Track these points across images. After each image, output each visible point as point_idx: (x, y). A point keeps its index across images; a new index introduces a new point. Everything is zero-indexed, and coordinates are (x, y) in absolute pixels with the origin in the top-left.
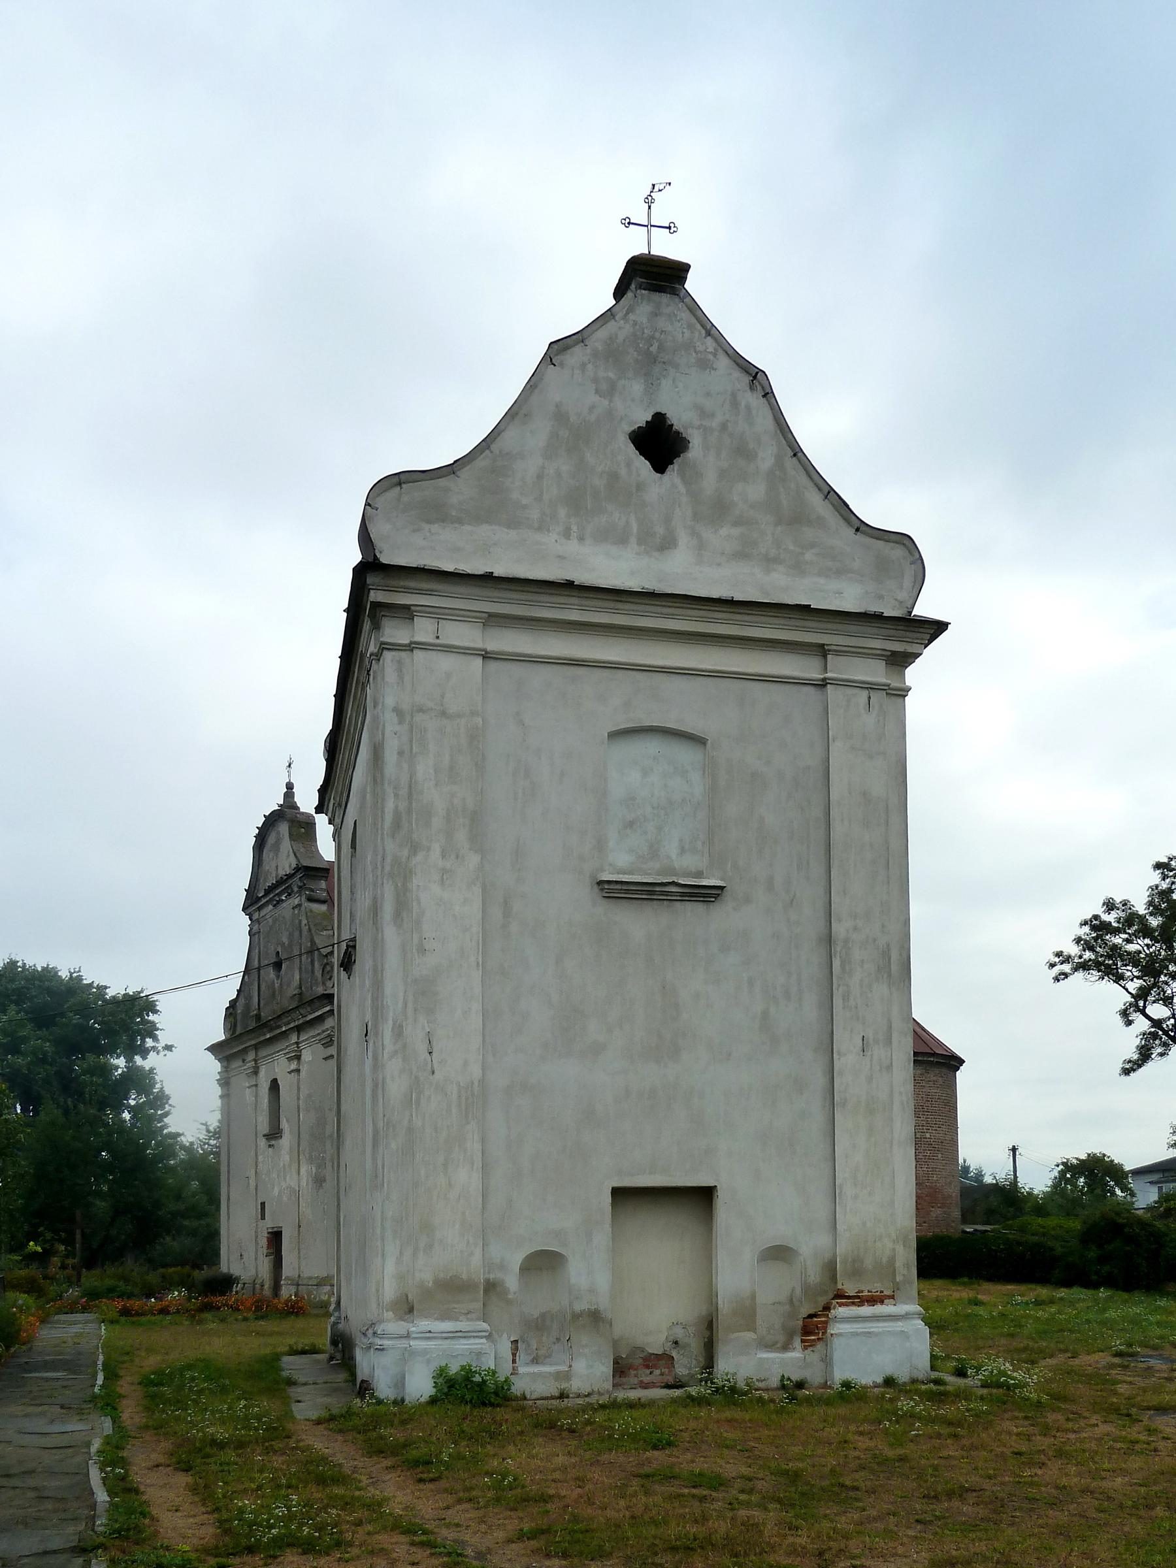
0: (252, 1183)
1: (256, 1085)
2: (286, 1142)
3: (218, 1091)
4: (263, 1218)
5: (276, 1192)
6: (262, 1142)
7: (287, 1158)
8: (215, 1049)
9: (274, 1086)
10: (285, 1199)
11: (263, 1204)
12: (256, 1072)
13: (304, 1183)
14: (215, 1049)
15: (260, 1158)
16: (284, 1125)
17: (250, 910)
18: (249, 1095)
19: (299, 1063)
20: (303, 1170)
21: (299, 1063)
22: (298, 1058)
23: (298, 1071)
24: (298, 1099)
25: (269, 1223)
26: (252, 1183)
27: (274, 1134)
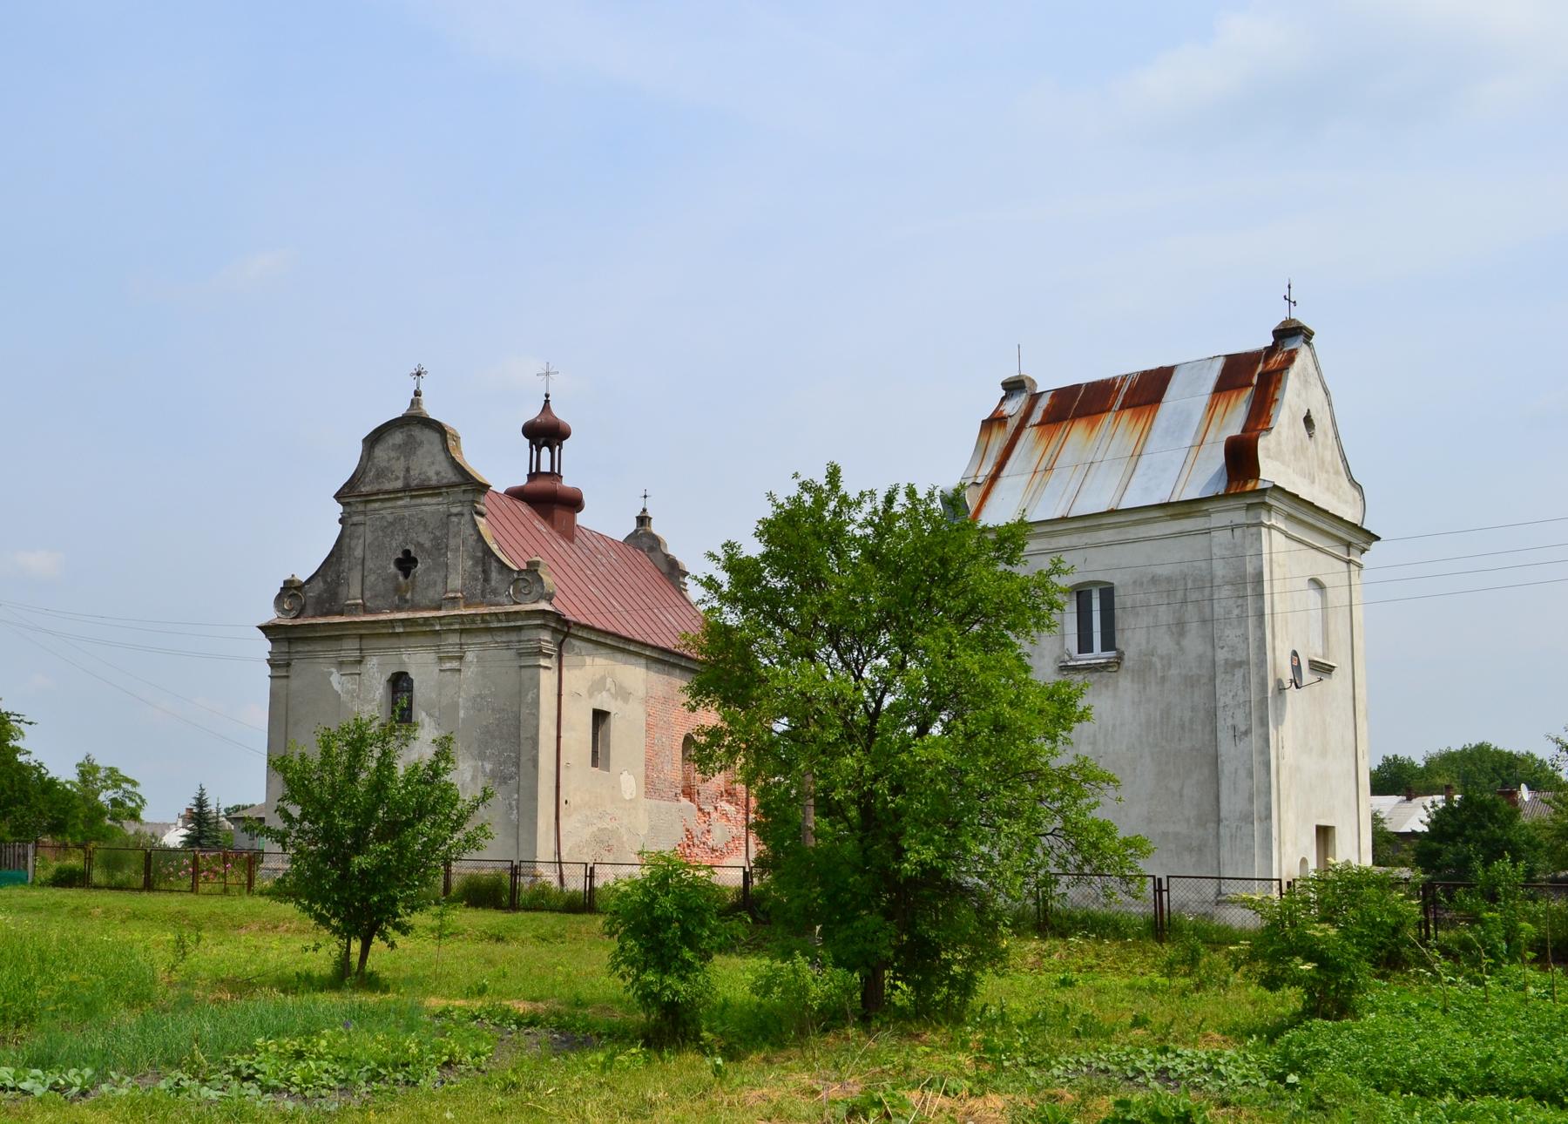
3: (268, 670)
22: (461, 658)
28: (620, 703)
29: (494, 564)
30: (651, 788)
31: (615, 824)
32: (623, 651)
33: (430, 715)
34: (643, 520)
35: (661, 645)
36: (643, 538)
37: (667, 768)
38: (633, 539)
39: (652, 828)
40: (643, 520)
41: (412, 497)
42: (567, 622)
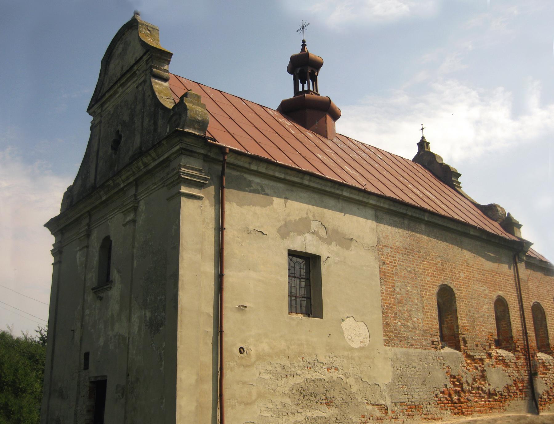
0: (77, 335)
1: (87, 247)
2: (115, 292)
3: (52, 259)
4: (86, 367)
5: (101, 342)
6: (90, 297)
7: (117, 307)
8: (52, 264)
9: (107, 245)
10: (111, 347)
11: (87, 355)
12: (88, 236)
13: (136, 329)
14: (52, 264)
15: (87, 312)
16: (115, 275)
17: (91, 111)
18: (79, 257)
19: (135, 214)
20: (135, 318)
21: (135, 214)
22: (135, 209)
23: (134, 221)
24: (133, 247)
25: (93, 372)
26: (77, 335)
27: (105, 281)
28: (334, 247)
29: (161, 112)
30: (392, 335)
31: (336, 375)
32: (337, 197)
33: (119, 272)
34: (423, 144)
35: (388, 194)
36: (425, 157)
37: (417, 317)
38: (415, 160)
39: (398, 376)
40: (423, 144)
41: (123, 85)
42: (222, 149)
